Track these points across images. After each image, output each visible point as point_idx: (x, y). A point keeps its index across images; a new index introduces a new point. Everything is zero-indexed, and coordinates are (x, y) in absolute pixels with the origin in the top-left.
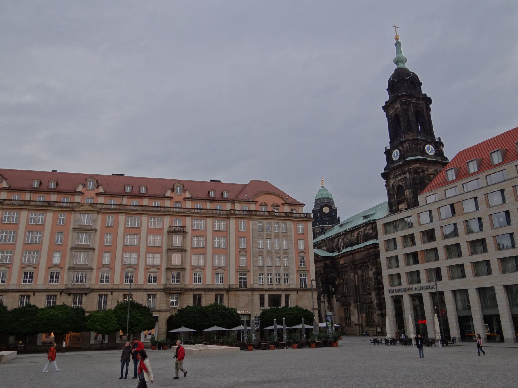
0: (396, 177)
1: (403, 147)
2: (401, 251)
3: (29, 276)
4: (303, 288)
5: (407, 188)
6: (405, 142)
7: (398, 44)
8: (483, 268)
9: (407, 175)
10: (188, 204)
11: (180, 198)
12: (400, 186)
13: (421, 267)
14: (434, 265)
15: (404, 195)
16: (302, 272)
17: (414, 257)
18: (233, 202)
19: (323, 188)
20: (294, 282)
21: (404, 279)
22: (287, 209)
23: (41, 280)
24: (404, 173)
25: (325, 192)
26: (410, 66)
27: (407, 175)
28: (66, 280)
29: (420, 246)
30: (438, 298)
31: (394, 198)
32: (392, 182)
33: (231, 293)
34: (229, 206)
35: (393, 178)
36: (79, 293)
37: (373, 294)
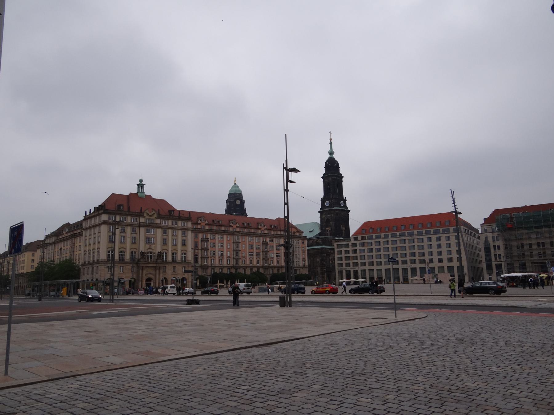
2: (343, 255)
3: (221, 261)
4: (304, 267)
7: (331, 143)
8: (371, 264)
10: (266, 232)
11: (263, 229)
13: (351, 262)
14: (356, 261)
16: (304, 260)
17: (348, 258)
18: (281, 231)
19: (235, 186)
20: (301, 265)
21: (344, 265)
22: (298, 234)
23: (225, 263)
24: (331, 214)
25: (237, 189)
26: (336, 157)
28: (232, 263)
29: (351, 254)
34: (279, 233)
36: (237, 268)
37: (319, 269)
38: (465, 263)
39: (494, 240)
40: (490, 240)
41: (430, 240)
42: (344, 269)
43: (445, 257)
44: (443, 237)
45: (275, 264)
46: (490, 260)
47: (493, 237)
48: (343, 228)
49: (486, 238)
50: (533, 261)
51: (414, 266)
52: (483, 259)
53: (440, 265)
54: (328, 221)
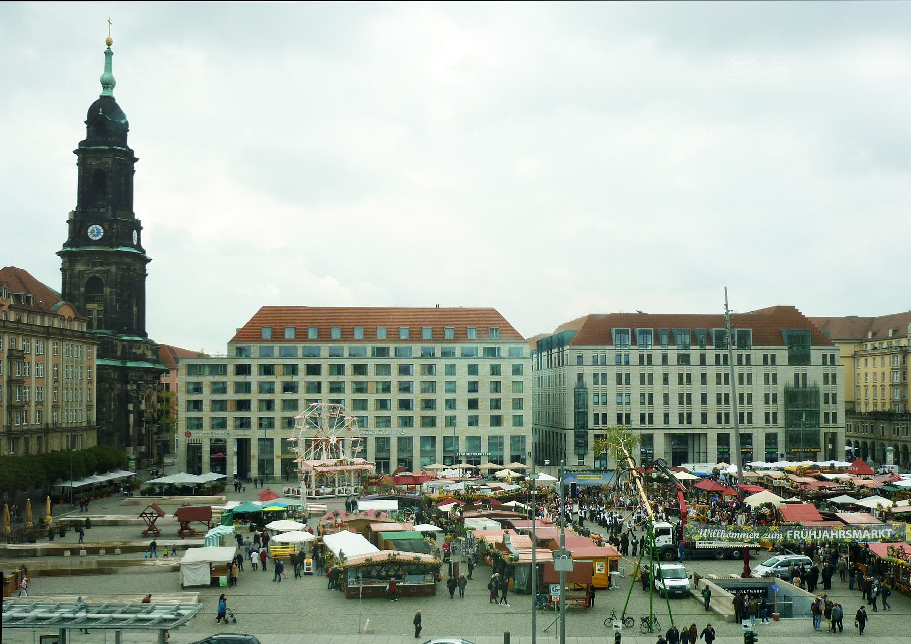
0: (94, 264)
1: (111, 226)
4: (89, 428)
5: (107, 286)
6: (117, 221)
9: (113, 269)
12: (95, 278)
15: (102, 292)
16: (89, 407)
17: (220, 405)
24: (108, 264)
26: (120, 96)
27: (113, 269)
30: (243, 444)
31: (79, 289)
32: (80, 267)
33: (50, 435)
35: (87, 264)
38: (527, 431)
39: (596, 383)
40: (588, 380)
41: (451, 370)
42: (205, 437)
43: (484, 412)
44: (484, 366)
45: (33, 422)
46: (584, 426)
47: (596, 376)
48: (135, 309)
49: (580, 377)
50: (667, 431)
51: (406, 432)
52: (571, 422)
53: (473, 431)
54: (95, 285)
